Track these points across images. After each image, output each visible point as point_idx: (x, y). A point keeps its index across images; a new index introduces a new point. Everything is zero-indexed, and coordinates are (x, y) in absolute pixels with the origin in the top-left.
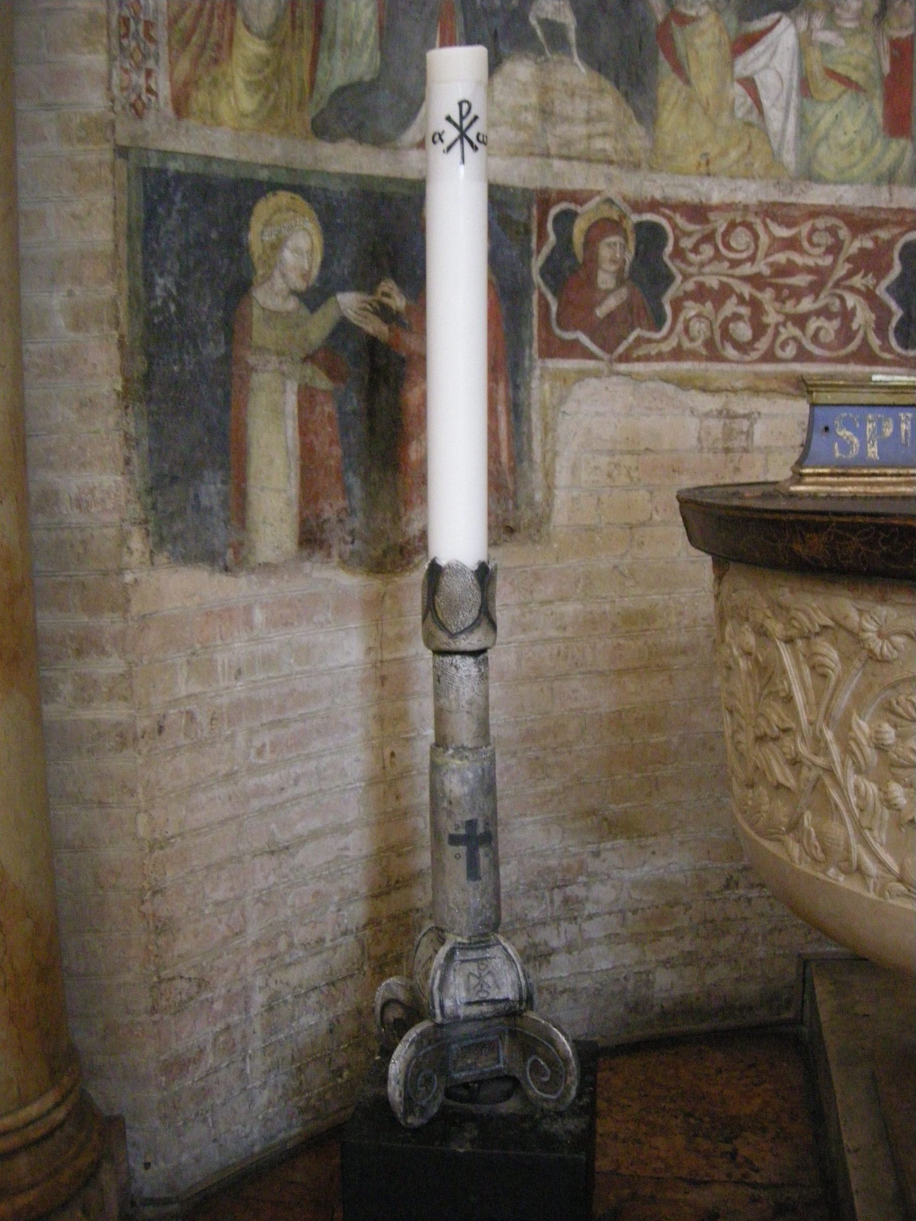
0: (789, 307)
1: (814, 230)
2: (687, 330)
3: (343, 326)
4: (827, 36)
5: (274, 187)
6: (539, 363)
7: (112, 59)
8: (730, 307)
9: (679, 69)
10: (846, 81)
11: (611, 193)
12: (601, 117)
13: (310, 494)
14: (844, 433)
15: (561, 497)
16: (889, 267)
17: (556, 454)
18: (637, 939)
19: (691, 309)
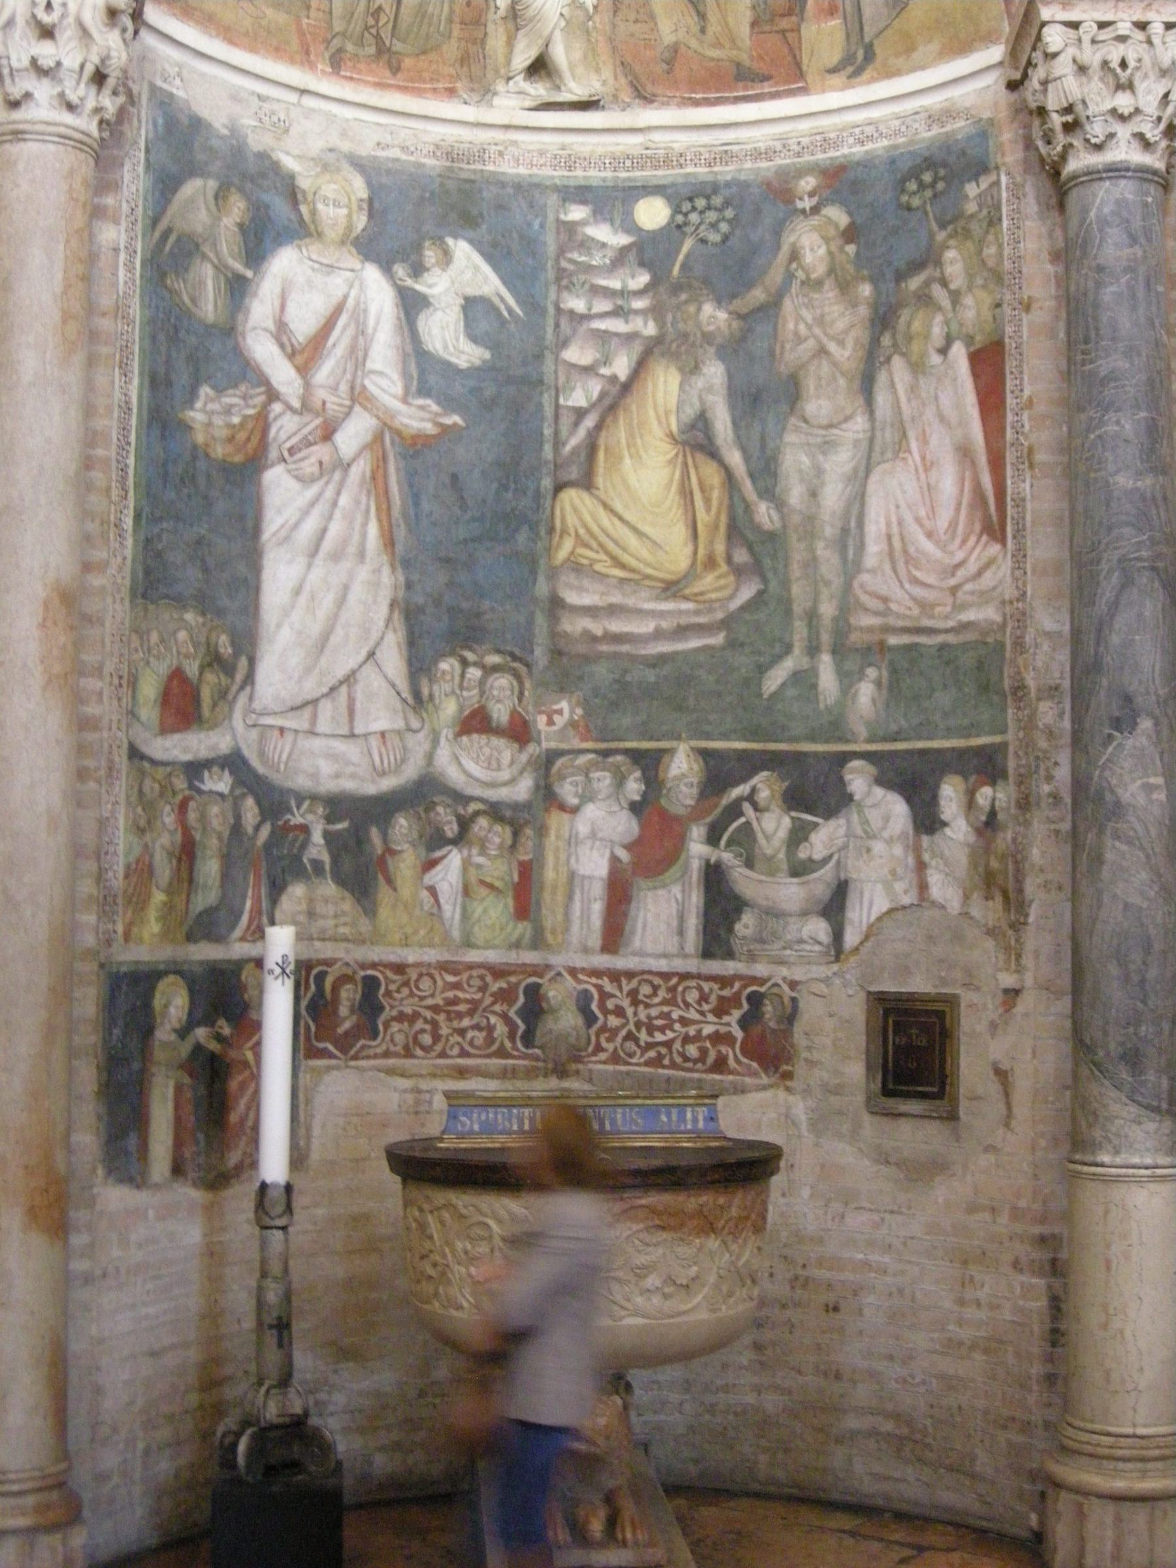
0: (455, 1024)
1: (471, 977)
2: (392, 1040)
3: (198, 1048)
4: (480, 860)
5: (166, 973)
6: (304, 1063)
7: (99, 918)
8: (419, 1025)
9: (390, 882)
10: (491, 886)
11: (348, 959)
12: (344, 913)
13: (178, 1144)
14: (463, 1119)
15: (315, 1144)
16: (517, 998)
17: (312, 1116)
18: (361, 1431)
19: (395, 1027)
